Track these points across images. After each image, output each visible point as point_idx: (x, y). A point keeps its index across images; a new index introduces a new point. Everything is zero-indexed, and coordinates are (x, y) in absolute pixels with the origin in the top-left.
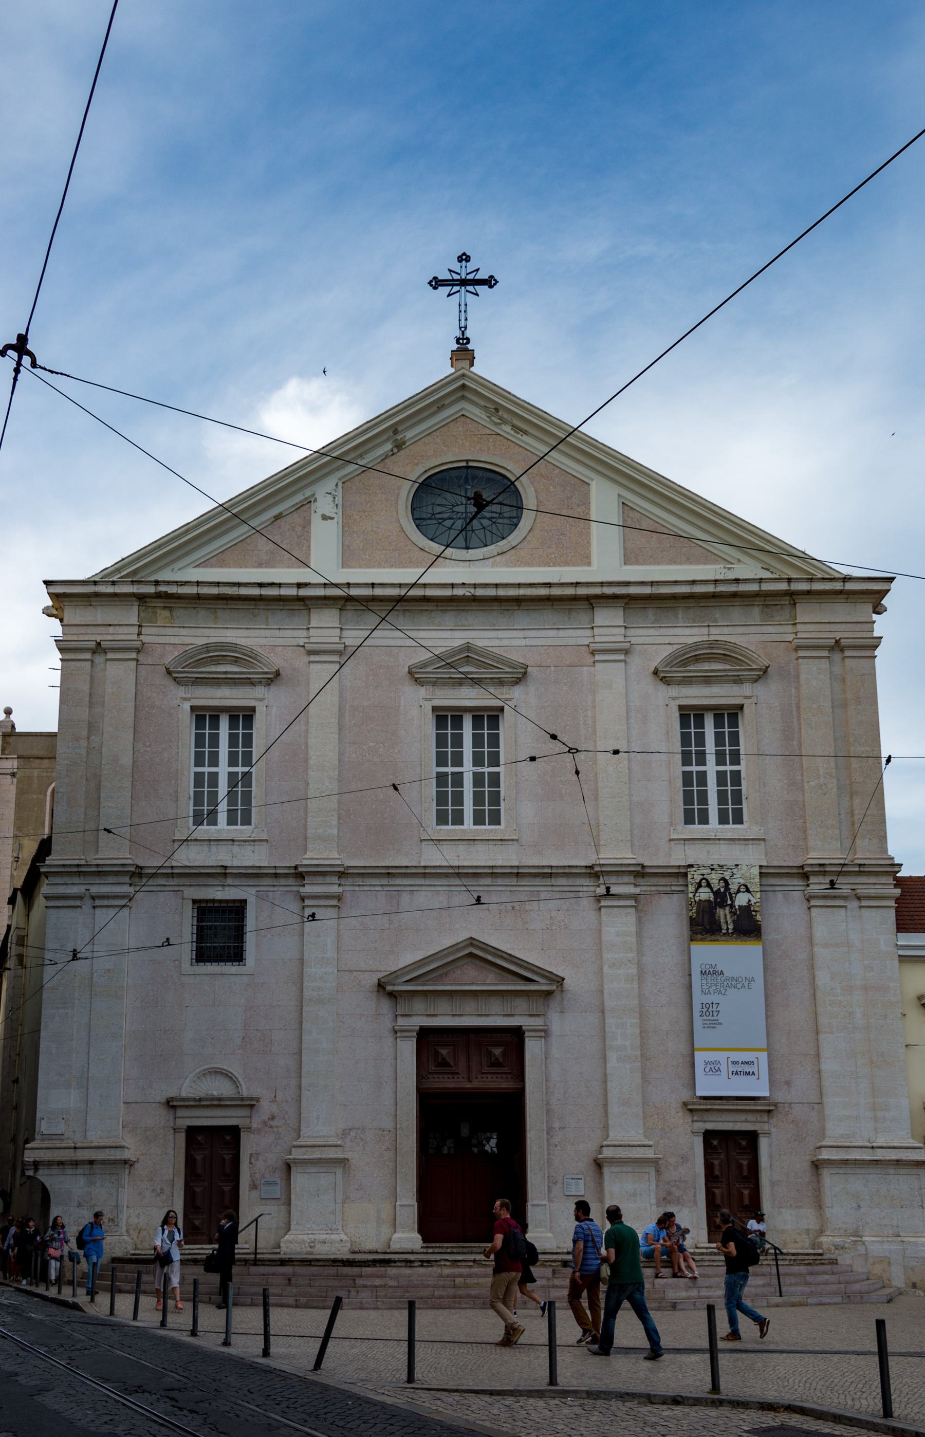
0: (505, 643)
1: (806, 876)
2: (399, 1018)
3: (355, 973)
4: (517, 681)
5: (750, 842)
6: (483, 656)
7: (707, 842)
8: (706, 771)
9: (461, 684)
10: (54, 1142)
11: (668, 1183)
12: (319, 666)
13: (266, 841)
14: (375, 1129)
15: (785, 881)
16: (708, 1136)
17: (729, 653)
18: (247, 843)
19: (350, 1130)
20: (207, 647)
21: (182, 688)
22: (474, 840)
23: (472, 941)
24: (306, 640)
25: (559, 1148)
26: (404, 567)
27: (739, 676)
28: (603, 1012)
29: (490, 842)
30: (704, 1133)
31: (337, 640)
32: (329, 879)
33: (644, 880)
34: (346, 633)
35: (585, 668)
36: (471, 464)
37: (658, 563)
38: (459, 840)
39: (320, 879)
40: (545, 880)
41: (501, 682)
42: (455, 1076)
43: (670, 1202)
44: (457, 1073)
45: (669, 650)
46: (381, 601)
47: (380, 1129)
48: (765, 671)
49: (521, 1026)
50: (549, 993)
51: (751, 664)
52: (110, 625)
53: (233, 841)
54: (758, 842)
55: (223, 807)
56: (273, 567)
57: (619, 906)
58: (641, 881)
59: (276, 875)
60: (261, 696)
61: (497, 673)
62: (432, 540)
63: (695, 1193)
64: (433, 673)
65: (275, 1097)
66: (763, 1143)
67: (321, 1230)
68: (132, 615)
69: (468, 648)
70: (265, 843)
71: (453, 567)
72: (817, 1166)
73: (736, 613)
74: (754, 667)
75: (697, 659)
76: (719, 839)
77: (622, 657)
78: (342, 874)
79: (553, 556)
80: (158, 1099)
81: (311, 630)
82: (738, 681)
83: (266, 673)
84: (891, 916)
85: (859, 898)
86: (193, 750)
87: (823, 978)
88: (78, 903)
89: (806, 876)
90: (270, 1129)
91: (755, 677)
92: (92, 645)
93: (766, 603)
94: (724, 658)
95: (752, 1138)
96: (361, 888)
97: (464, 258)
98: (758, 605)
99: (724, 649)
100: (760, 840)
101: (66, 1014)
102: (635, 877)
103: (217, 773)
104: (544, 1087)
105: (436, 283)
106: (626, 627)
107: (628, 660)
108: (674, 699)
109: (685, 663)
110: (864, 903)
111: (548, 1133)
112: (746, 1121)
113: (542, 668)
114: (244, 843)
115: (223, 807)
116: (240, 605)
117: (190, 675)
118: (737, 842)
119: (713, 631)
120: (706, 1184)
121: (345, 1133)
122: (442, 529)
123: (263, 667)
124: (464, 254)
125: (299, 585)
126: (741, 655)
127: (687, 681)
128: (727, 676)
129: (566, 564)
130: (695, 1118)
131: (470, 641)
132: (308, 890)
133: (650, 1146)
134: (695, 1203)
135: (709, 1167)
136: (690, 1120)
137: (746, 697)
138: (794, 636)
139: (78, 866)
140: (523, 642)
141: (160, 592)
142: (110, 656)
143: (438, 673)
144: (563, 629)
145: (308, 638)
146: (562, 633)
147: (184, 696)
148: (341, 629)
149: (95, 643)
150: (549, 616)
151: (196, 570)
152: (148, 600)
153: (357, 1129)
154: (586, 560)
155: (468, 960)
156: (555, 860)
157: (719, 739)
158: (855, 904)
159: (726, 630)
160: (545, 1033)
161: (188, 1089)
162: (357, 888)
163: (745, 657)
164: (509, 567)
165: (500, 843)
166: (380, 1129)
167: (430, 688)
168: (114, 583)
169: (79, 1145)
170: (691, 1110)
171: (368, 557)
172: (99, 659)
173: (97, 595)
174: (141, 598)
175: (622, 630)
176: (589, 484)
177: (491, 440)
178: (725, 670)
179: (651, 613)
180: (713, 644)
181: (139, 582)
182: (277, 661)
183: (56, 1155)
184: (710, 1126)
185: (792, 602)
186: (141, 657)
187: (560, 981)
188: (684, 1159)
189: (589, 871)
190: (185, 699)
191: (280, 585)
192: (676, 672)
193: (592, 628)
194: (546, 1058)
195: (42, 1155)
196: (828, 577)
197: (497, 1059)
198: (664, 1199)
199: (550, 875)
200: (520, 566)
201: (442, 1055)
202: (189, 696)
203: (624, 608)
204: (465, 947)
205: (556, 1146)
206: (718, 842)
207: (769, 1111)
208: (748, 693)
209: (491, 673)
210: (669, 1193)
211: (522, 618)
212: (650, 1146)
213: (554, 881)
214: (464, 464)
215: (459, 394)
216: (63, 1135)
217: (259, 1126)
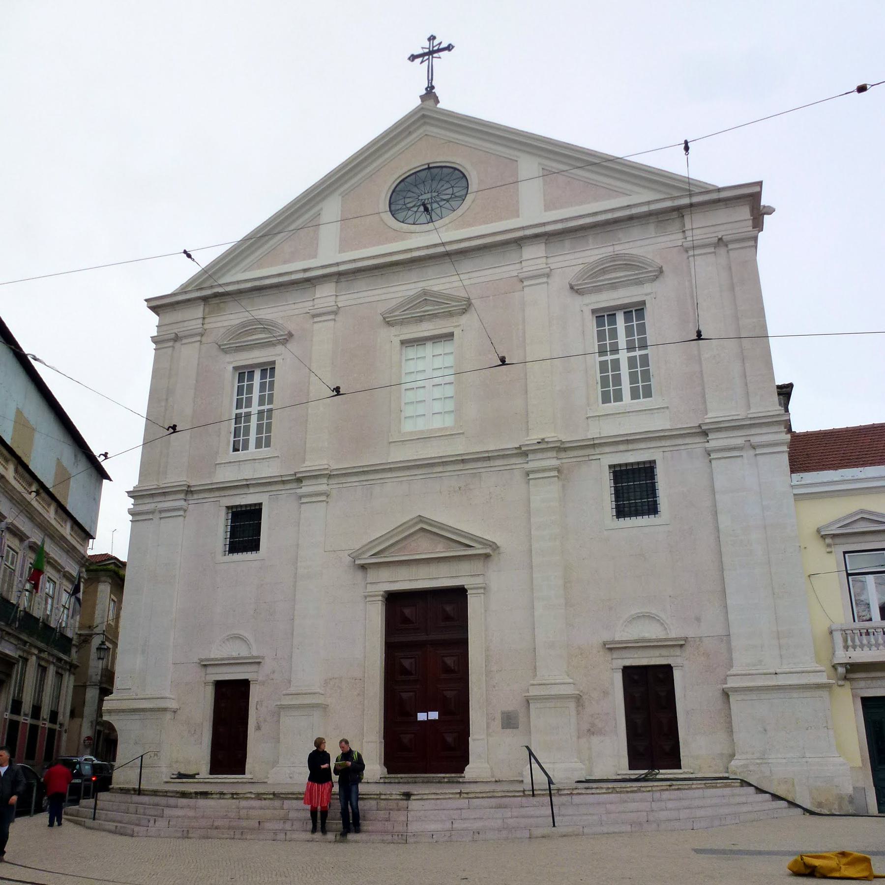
1: (705, 433)
2: (368, 585)
4: (464, 311)
5: (655, 411)
6: (436, 297)
8: (619, 359)
9: (421, 321)
11: (592, 716)
12: (320, 325)
15: (687, 441)
16: (628, 672)
17: (628, 263)
18: (265, 460)
20: (243, 325)
21: (228, 356)
23: (421, 519)
25: (497, 688)
27: (639, 278)
28: (532, 568)
30: (623, 670)
31: (333, 303)
32: (320, 481)
33: (566, 453)
34: (340, 298)
36: (431, 166)
38: (418, 439)
39: (313, 482)
40: (485, 462)
41: (451, 314)
43: (593, 734)
45: (582, 266)
46: (364, 271)
48: (661, 271)
49: (464, 586)
50: (487, 556)
51: (646, 266)
53: (255, 460)
54: (662, 410)
57: (543, 478)
58: (563, 455)
59: (283, 482)
61: (447, 307)
62: (403, 222)
64: (401, 315)
66: (677, 674)
68: (198, 311)
69: (425, 292)
70: (277, 459)
72: (726, 694)
73: (636, 232)
74: (650, 269)
75: (604, 271)
76: (629, 412)
77: (545, 280)
81: (315, 300)
82: (639, 282)
83: (282, 335)
84: (785, 459)
85: (754, 448)
87: (724, 521)
88: (151, 516)
89: (705, 433)
91: (652, 277)
92: (173, 336)
93: (660, 219)
94: (628, 266)
96: (344, 485)
98: (653, 223)
99: (625, 260)
100: (663, 408)
102: (557, 452)
106: (547, 257)
107: (550, 282)
108: (587, 305)
110: (758, 451)
112: (661, 656)
116: (269, 292)
117: (232, 346)
118: (644, 412)
119: (617, 248)
122: (410, 213)
123: (280, 331)
125: (305, 270)
126: (640, 262)
127: (598, 289)
128: (629, 280)
129: (501, 219)
130: (614, 656)
131: (426, 288)
132: (305, 490)
136: (610, 659)
137: (646, 295)
138: (684, 240)
141: (215, 293)
142: (184, 341)
143: (404, 315)
144: (498, 267)
145: (314, 306)
146: (497, 270)
148: (337, 296)
149: (174, 334)
150: (488, 259)
152: (210, 300)
155: (422, 534)
156: (492, 445)
157: (629, 331)
158: (752, 452)
159: (627, 246)
161: (217, 652)
162: (341, 486)
163: (643, 263)
167: (398, 327)
168: (186, 292)
170: (610, 649)
172: (178, 345)
173: (178, 303)
174: (205, 299)
175: (544, 260)
176: (517, 161)
178: (625, 276)
179: (567, 243)
181: (201, 289)
182: (291, 327)
184: (628, 663)
185: (681, 215)
186: (204, 339)
187: (495, 547)
188: (606, 693)
189: (518, 451)
190: (229, 363)
191: (291, 273)
192: (586, 283)
193: (521, 262)
194: (486, 611)
196: (704, 190)
199: (489, 458)
202: (232, 360)
203: (545, 243)
204: (416, 523)
205: (494, 687)
206: (627, 414)
207: (681, 646)
209: (442, 308)
211: (466, 265)
213: (492, 463)
214: (427, 166)
215: (422, 121)
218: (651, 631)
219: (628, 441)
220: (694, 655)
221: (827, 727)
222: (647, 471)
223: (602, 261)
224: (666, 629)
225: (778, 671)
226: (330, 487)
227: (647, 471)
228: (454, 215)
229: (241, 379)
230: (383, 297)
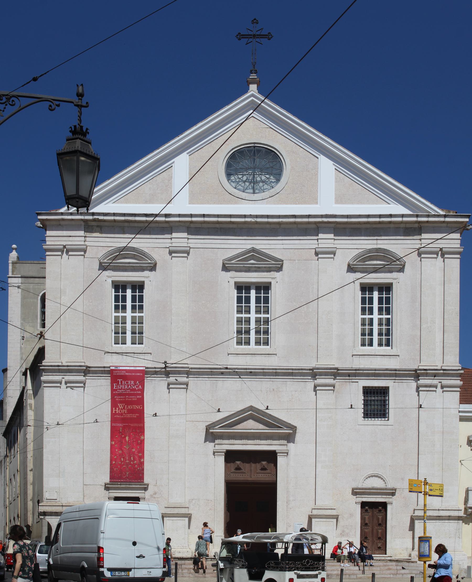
0: (272, 247)
3: (195, 422)
5: (392, 357)
7: (371, 356)
10: (52, 503)
11: (343, 526)
13: (151, 353)
14: (204, 500)
16: (363, 505)
18: (141, 354)
19: (192, 500)
22: (255, 354)
24: (170, 245)
25: (292, 510)
26: (221, 204)
29: (263, 355)
30: (361, 503)
35: (313, 261)
37: (352, 203)
41: (269, 270)
42: (244, 474)
44: (245, 473)
45: (357, 252)
47: (207, 500)
52: (70, 236)
53: (134, 353)
55: (129, 335)
56: (153, 203)
60: (147, 275)
61: (268, 264)
63: (356, 531)
65: (156, 483)
66: (389, 507)
67: (178, 547)
69: (253, 250)
71: (246, 204)
75: (371, 258)
76: (377, 355)
78: (188, 373)
79: (298, 198)
80: (100, 483)
86: (113, 304)
90: (154, 499)
95: (384, 505)
97: (255, 21)
101: (55, 441)
103: (126, 316)
104: (286, 480)
105: (240, 36)
109: (364, 260)
111: (287, 503)
113: (291, 261)
114: (139, 355)
115: (129, 335)
120: (361, 527)
121: (190, 501)
123: (148, 260)
124: (255, 19)
125: (166, 216)
131: (254, 246)
133: (334, 509)
134: (355, 535)
135: (363, 518)
139: (58, 366)
140: (282, 247)
147: (108, 275)
149: (62, 246)
151: (114, 205)
153: (196, 499)
154: (315, 201)
160: (287, 453)
164: (275, 204)
165: (268, 356)
166: (207, 500)
169: (63, 505)
171: (202, 198)
177: (267, 131)
180: (378, 250)
183: (53, 509)
184: (365, 500)
187: (294, 428)
188: (351, 515)
193: (318, 240)
194: (287, 466)
195: (47, 509)
197: (264, 466)
198: (341, 534)
200: (281, 204)
201: (237, 464)
205: (291, 508)
206: (376, 356)
208: (395, 277)
210: (343, 531)
212: (334, 509)
216: (56, 499)
217: (149, 497)
218: (377, 483)
219: (375, 374)
220: (399, 498)
221: (459, 537)
222: (384, 391)
223: (370, 251)
224: (386, 483)
225: (440, 509)
226: (190, 379)
227: (384, 391)
228: (272, 191)
229: (117, 290)
230: (223, 246)
